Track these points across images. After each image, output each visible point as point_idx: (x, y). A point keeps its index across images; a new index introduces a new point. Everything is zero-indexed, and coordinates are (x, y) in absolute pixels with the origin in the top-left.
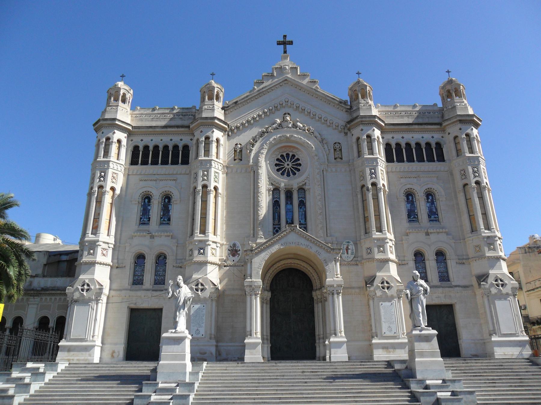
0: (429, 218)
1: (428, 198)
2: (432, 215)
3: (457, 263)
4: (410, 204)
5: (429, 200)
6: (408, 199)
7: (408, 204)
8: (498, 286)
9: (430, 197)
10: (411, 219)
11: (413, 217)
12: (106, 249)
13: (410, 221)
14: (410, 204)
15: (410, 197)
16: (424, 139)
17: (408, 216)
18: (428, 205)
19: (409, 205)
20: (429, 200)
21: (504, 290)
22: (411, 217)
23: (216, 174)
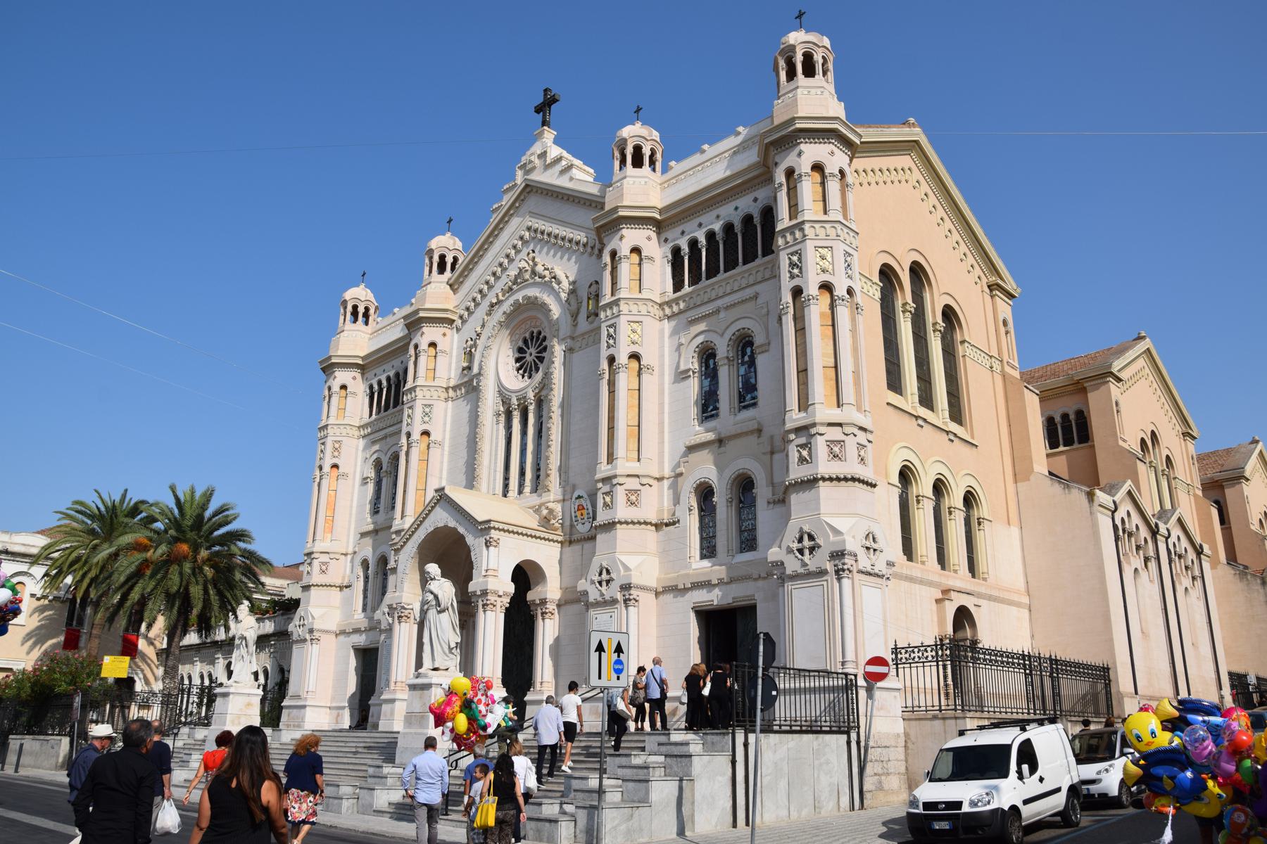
0: (740, 402)
1: (744, 354)
2: (748, 393)
3: (769, 503)
4: (709, 380)
5: (746, 358)
6: (707, 366)
7: (706, 378)
8: (802, 554)
9: (748, 350)
10: (709, 414)
11: (711, 407)
12: (326, 563)
13: (707, 418)
14: (709, 380)
15: (711, 362)
16: (739, 210)
17: (703, 408)
18: (742, 370)
19: (707, 383)
20: (746, 358)
21: (812, 562)
22: (709, 409)
23: (427, 410)
